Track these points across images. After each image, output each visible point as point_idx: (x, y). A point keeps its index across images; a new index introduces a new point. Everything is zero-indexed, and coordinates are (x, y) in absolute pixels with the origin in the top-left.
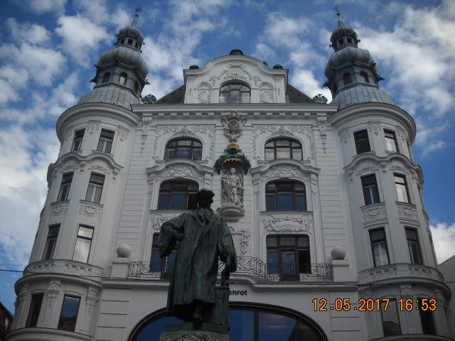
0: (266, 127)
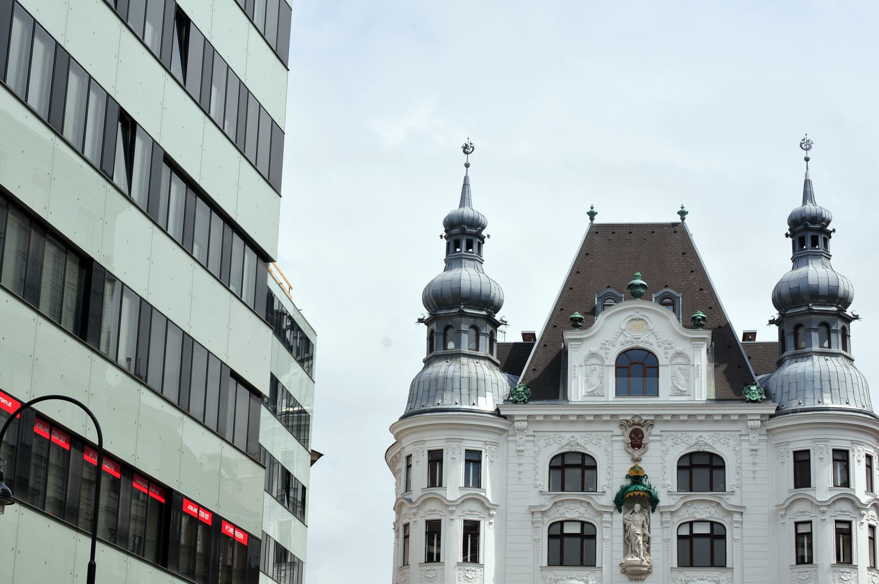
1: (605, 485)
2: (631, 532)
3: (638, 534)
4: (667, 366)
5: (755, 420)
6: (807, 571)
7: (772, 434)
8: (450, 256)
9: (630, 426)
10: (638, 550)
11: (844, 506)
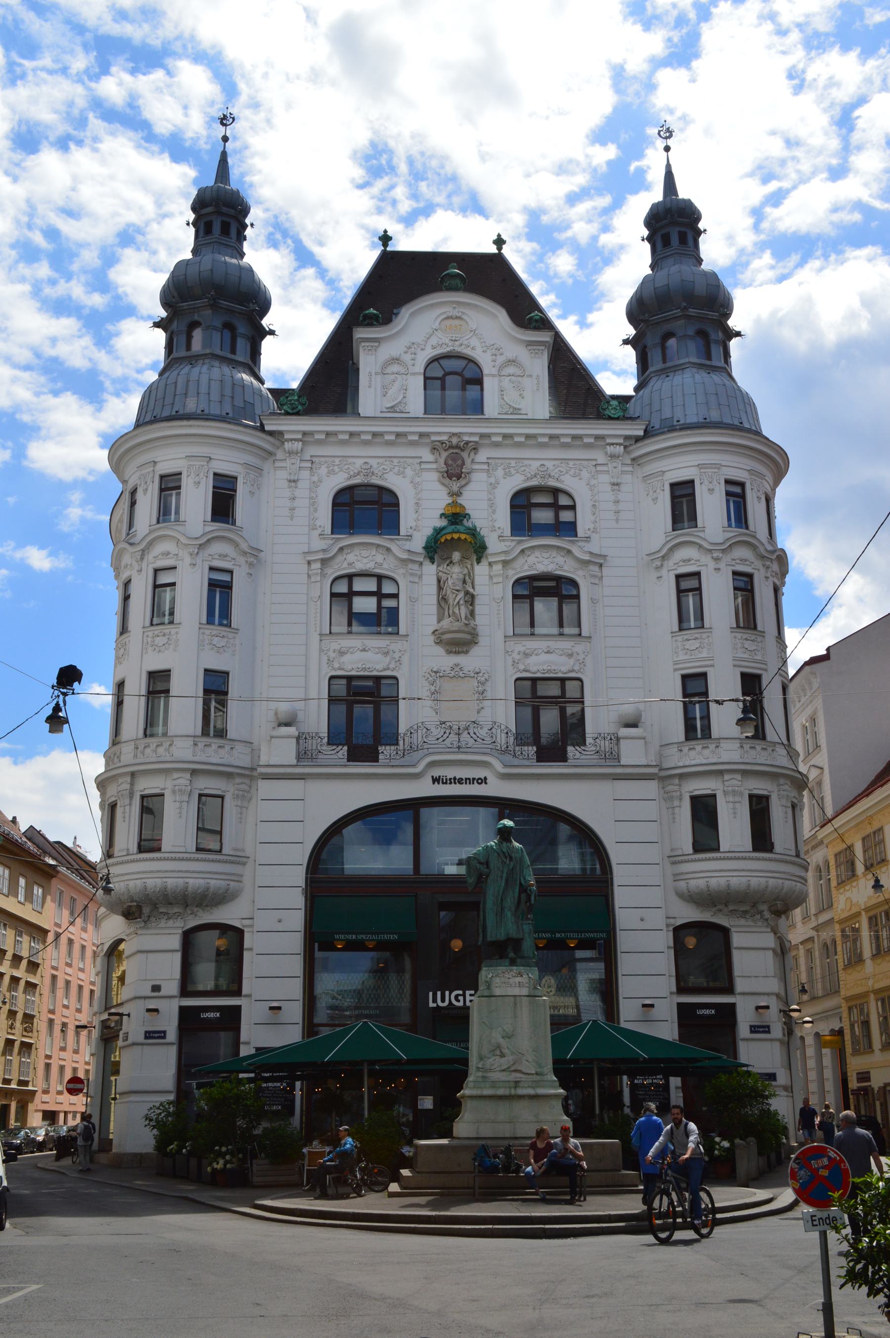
0: (513, 463)
1: (411, 528)
2: (448, 589)
3: (458, 591)
4: (493, 376)
5: (617, 444)
6: (696, 639)
7: (639, 465)
8: (201, 241)
9: (445, 450)
10: (457, 612)
11: (742, 552)
